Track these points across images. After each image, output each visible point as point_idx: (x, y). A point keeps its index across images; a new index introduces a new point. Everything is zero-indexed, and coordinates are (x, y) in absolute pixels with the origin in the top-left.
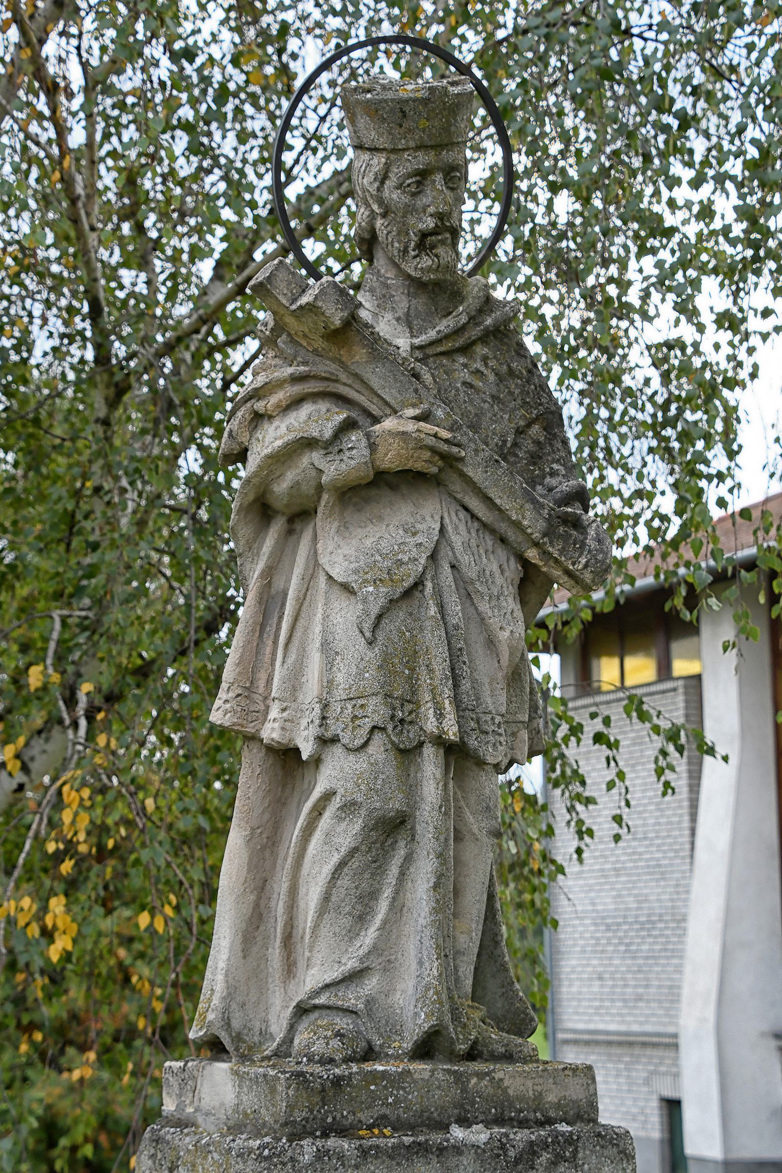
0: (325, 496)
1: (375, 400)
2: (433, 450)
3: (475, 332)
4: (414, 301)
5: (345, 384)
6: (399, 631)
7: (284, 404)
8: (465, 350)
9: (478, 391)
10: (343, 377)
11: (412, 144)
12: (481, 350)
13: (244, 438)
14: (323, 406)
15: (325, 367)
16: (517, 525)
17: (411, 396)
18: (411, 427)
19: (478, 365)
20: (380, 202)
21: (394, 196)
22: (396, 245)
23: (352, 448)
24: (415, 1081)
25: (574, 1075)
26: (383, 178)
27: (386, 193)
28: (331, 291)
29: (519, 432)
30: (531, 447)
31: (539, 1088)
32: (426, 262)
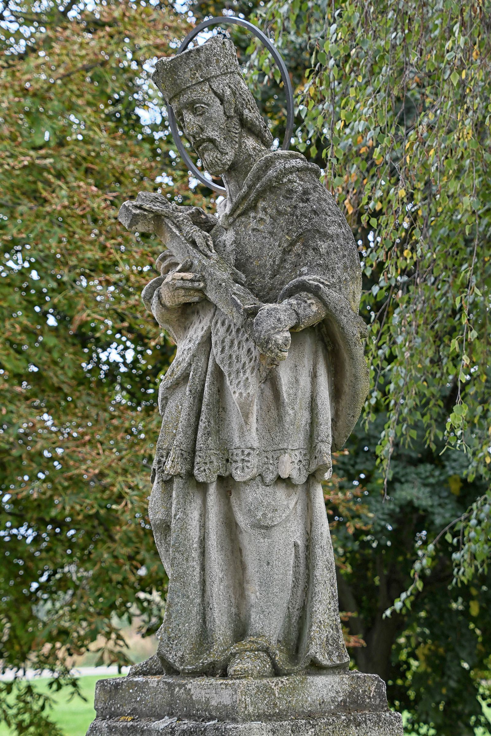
3: (252, 196)
8: (253, 207)
19: (260, 215)
24: (150, 688)
25: (226, 688)
29: (286, 252)
31: (208, 696)
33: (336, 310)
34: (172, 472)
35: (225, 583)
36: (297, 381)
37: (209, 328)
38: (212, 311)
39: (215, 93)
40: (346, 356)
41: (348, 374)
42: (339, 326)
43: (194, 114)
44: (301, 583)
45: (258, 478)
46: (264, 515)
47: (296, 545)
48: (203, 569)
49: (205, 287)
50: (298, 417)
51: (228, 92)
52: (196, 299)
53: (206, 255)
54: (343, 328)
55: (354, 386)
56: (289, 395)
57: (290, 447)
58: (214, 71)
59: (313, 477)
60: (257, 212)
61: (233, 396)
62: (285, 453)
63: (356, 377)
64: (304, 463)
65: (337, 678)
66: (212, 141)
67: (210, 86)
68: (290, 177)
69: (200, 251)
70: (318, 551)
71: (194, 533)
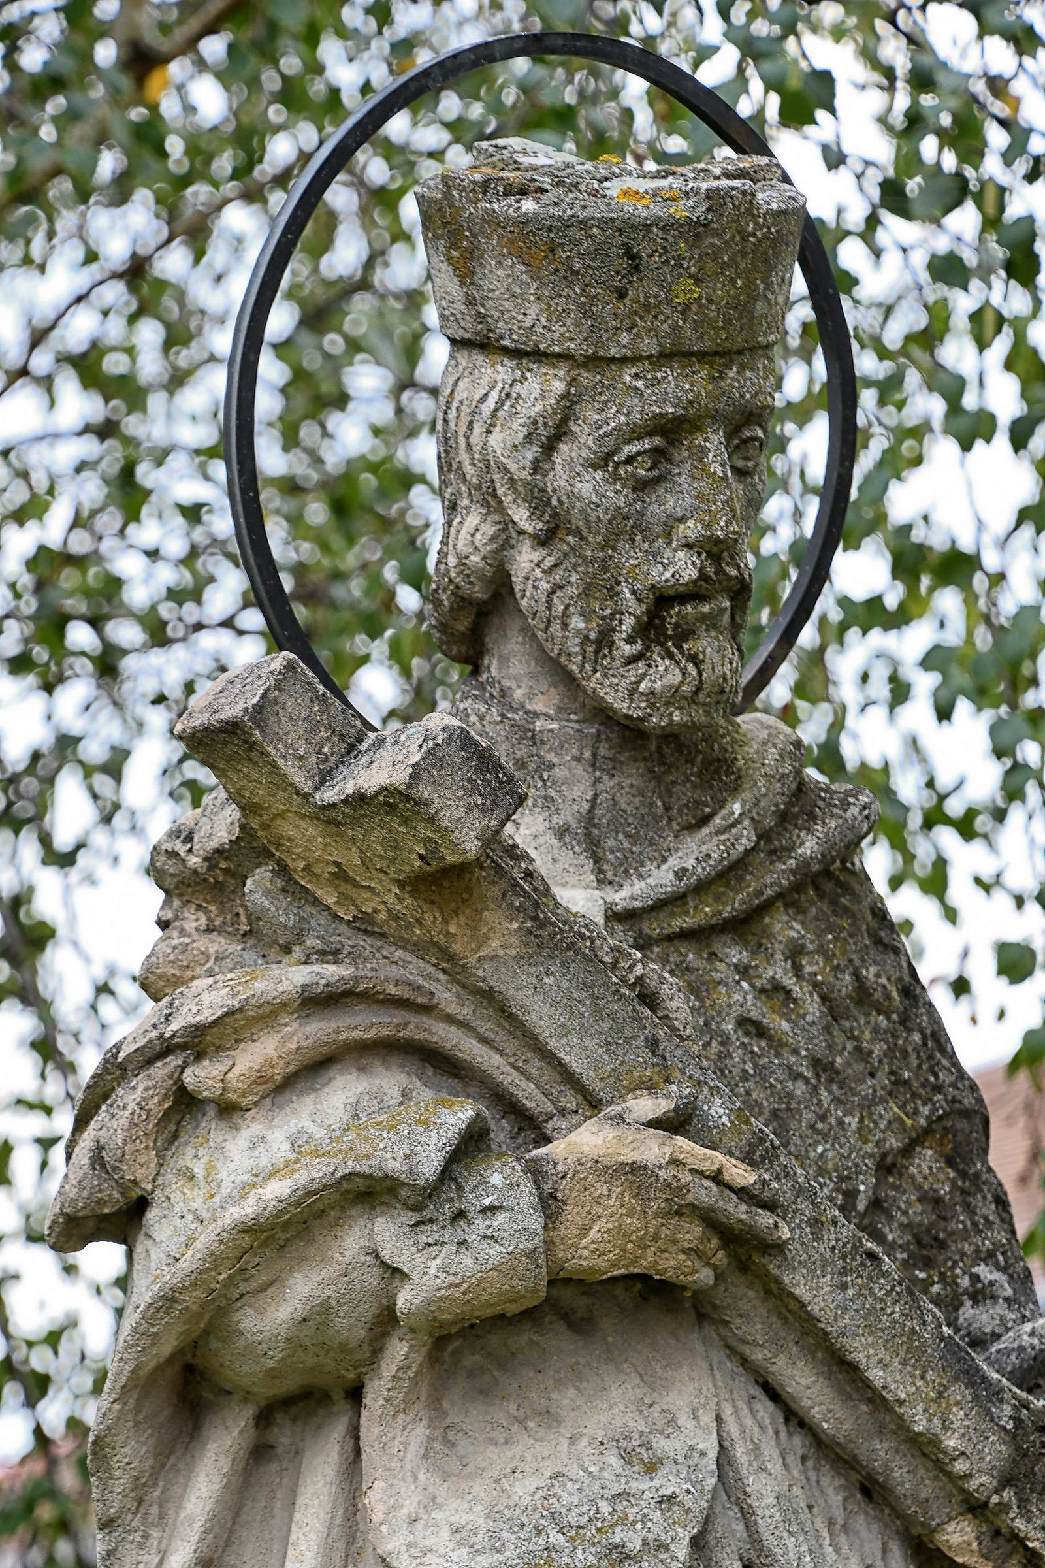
0: (398, 1351)
1: (535, 1066)
2: (710, 1220)
3: (775, 876)
4: (608, 783)
5: (450, 1019)
7: (278, 1073)
8: (744, 926)
9: (776, 1044)
10: (446, 997)
11: (650, 346)
12: (786, 928)
13: (141, 1170)
14: (390, 1081)
15: (398, 969)
16: (925, 1449)
17: (637, 1057)
18: (654, 1149)
19: (779, 970)
20: (538, 500)
21: (585, 488)
22: (577, 623)
23: (492, 1209)
26: (552, 435)
27: (559, 477)
28: (453, 755)
29: (886, 1167)
30: (917, 1213)
32: (664, 674)
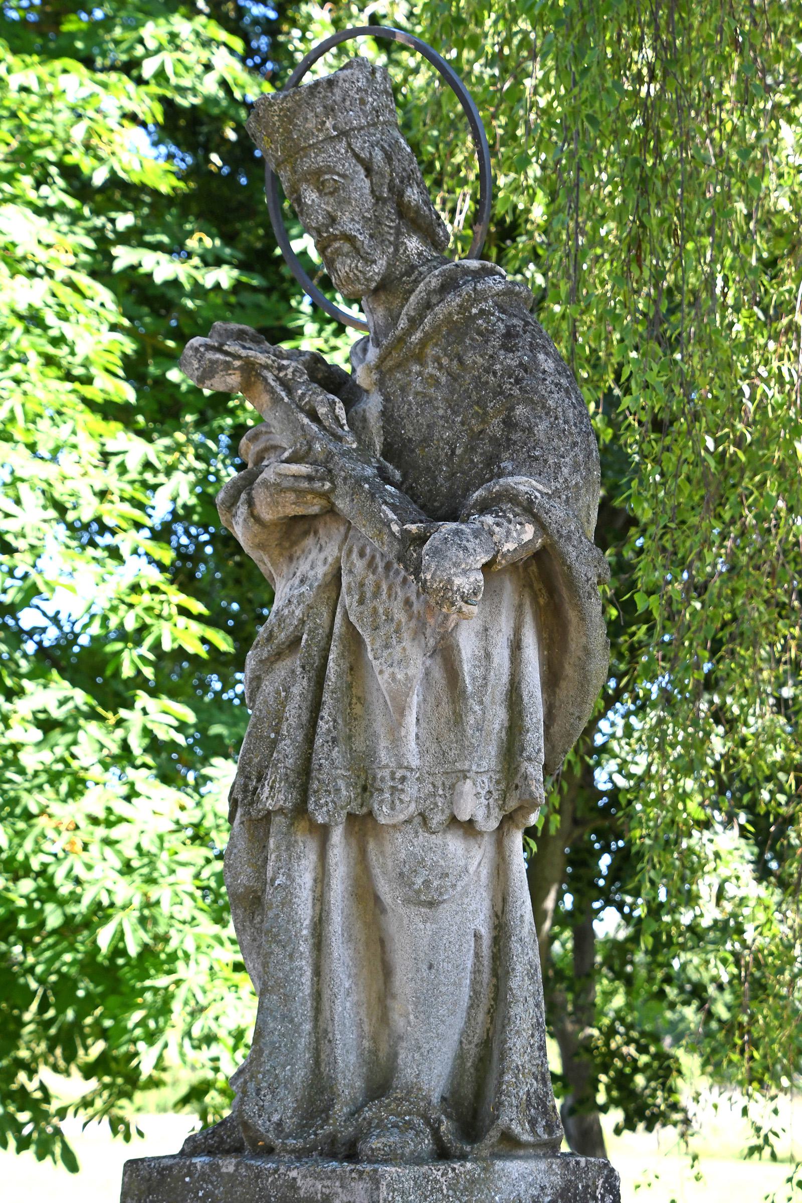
6: (278, 692)
19: (431, 369)
30: (488, 448)
31: (327, 1191)
33: (561, 536)
34: (270, 805)
35: (354, 998)
36: (488, 656)
37: (338, 560)
38: (342, 529)
39: (357, 156)
40: (572, 615)
41: (573, 646)
42: (564, 563)
43: (319, 191)
44: (485, 1003)
45: (417, 820)
46: (427, 883)
47: (477, 936)
48: (317, 972)
49: (333, 490)
50: (489, 716)
51: (378, 155)
52: (315, 509)
53: (334, 435)
54: (570, 567)
55: (582, 668)
56: (474, 679)
57: (474, 768)
58: (355, 119)
59: (508, 820)
60: (423, 364)
61: (379, 677)
62: (465, 777)
63: (587, 651)
64: (496, 795)
65: (543, 1165)
66: (349, 239)
67: (349, 145)
68: (483, 305)
69: (325, 428)
70: (515, 947)
71: (305, 911)
